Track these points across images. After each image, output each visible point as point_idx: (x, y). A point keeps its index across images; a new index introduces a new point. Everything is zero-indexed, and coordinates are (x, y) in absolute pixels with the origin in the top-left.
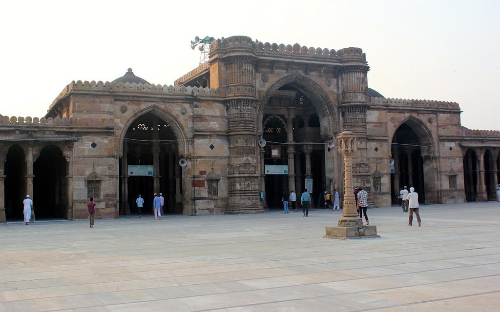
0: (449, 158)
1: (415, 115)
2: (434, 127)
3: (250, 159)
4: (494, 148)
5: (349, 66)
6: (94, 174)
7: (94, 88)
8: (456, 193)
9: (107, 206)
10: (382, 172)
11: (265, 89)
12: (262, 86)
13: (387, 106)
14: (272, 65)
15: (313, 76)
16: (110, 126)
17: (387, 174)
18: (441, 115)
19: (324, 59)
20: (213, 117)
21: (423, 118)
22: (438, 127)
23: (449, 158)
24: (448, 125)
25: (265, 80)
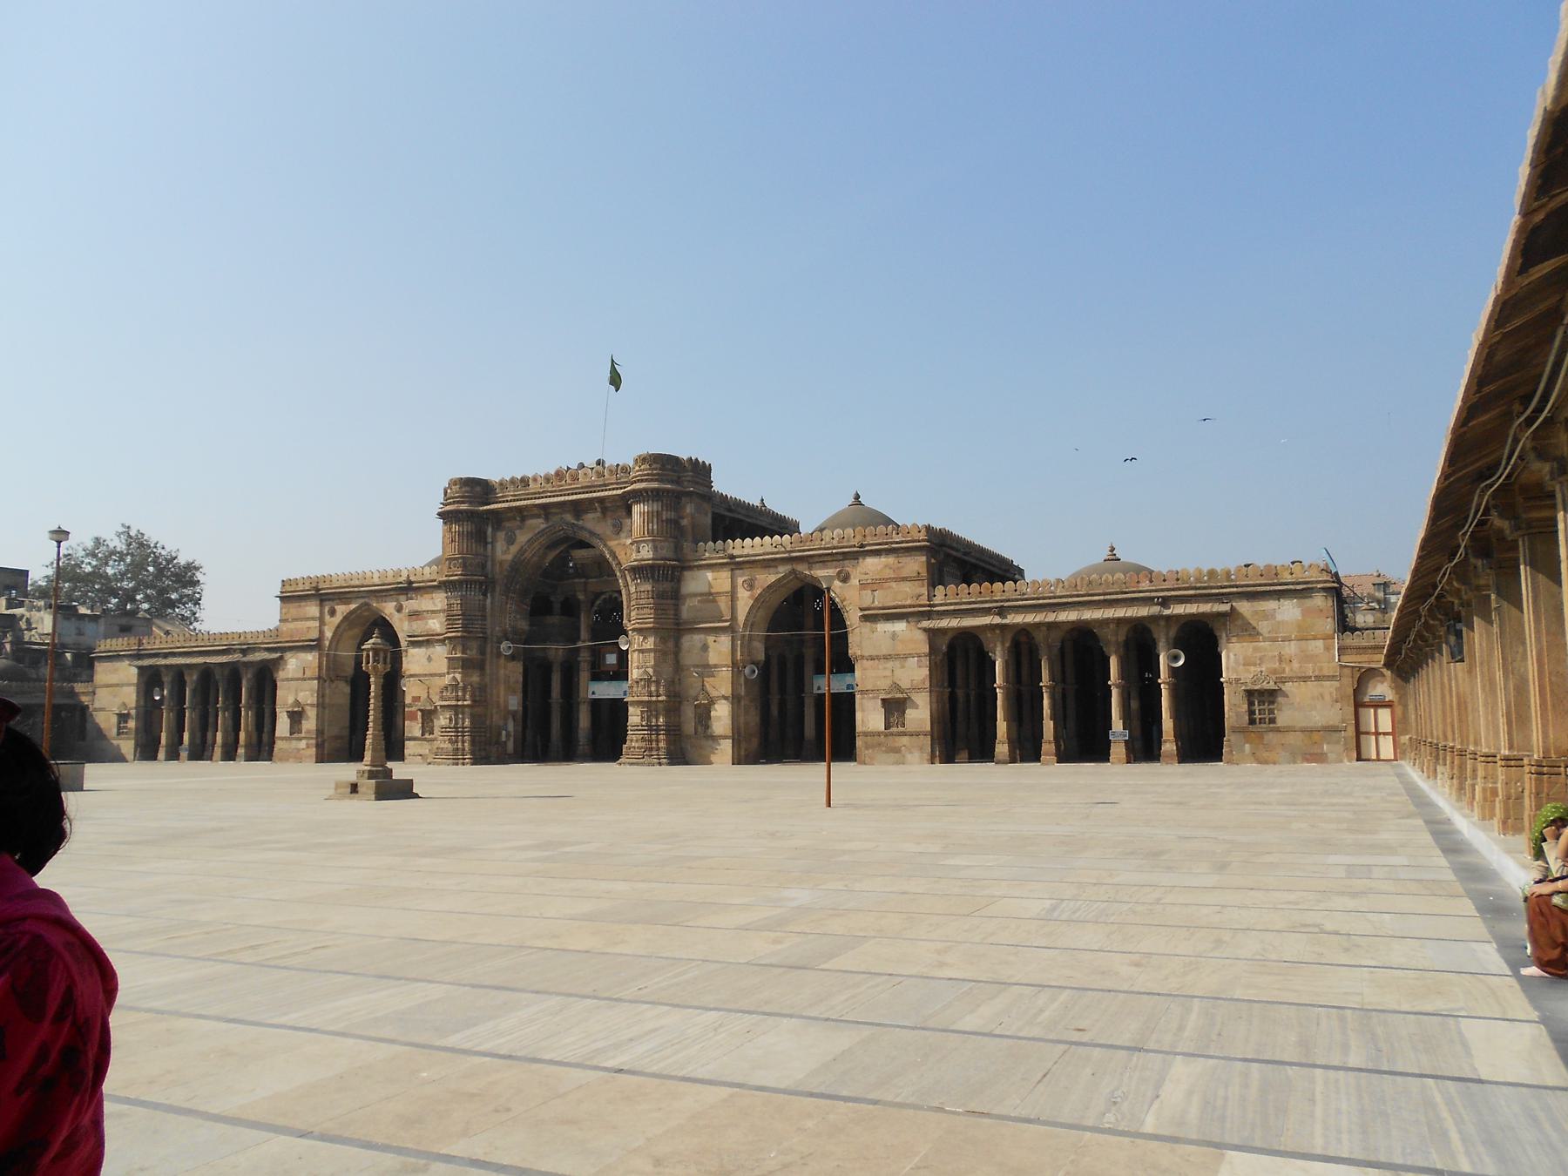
0: (887, 658)
1: (802, 568)
2: (850, 594)
3: (458, 677)
4: (1038, 625)
5: (634, 491)
6: (297, 703)
8: (905, 740)
9: (308, 746)
10: (714, 693)
11: (509, 557)
12: (506, 552)
13: (732, 557)
14: (522, 514)
15: (591, 521)
16: (315, 635)
17: (726, 698)
18: (870, 561)
19: (604, 487)
20: (433, 612)
21: (821, 573)
22: (863, 586)
23: (887, 658)
24: (886, 580)
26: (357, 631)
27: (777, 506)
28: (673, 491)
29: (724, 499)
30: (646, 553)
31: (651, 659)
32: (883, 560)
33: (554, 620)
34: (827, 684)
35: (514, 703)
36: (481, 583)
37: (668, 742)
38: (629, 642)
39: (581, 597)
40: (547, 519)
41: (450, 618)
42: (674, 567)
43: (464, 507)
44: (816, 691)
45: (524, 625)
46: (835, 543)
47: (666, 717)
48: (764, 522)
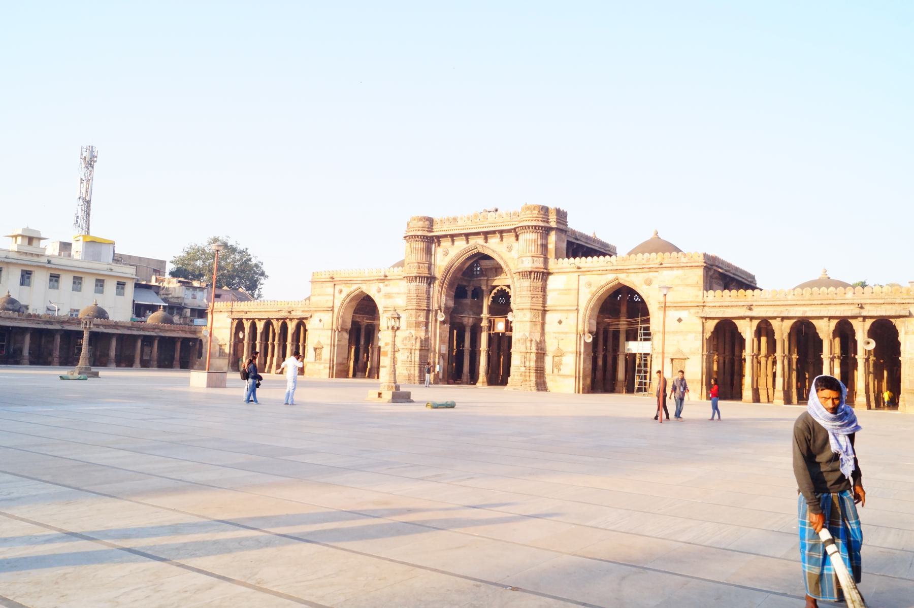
7: (323, 276)
13: (579, 268)
18: (666, 273)
25: (446, 253)
26: (354, 304)
27: (604, 236)
28: (545, 227)
29: (574, 232)
30: (528, 264)
31: (528, 326)
32: (676, 272)
33: (468, 301)
34: (635, 347)
35: (445, 349)
36: (428, 278)
37: (537, 377)
38: (514, 316)
39: (484, 288)
40: (468, 242)
41: (409, 299)
42: (543, 273)
43: (420, 233)
44: (626, 351)
45: (451, 304)
46: (644, 262)
47: (537, 361)
48: (596, 247)
